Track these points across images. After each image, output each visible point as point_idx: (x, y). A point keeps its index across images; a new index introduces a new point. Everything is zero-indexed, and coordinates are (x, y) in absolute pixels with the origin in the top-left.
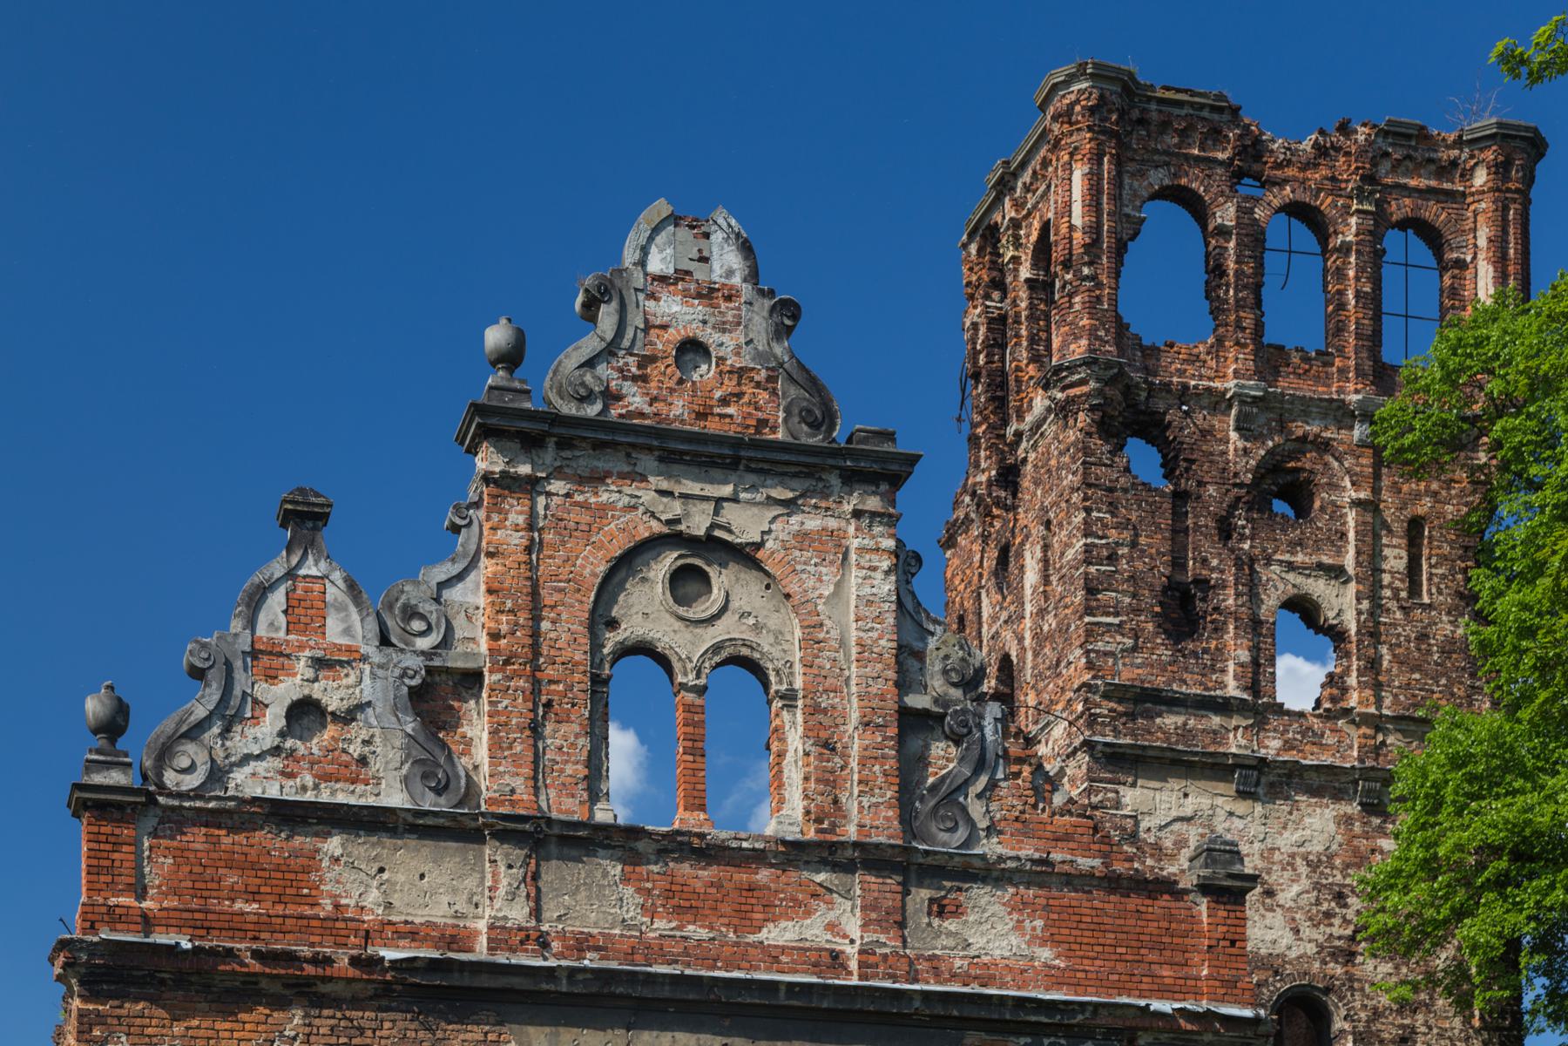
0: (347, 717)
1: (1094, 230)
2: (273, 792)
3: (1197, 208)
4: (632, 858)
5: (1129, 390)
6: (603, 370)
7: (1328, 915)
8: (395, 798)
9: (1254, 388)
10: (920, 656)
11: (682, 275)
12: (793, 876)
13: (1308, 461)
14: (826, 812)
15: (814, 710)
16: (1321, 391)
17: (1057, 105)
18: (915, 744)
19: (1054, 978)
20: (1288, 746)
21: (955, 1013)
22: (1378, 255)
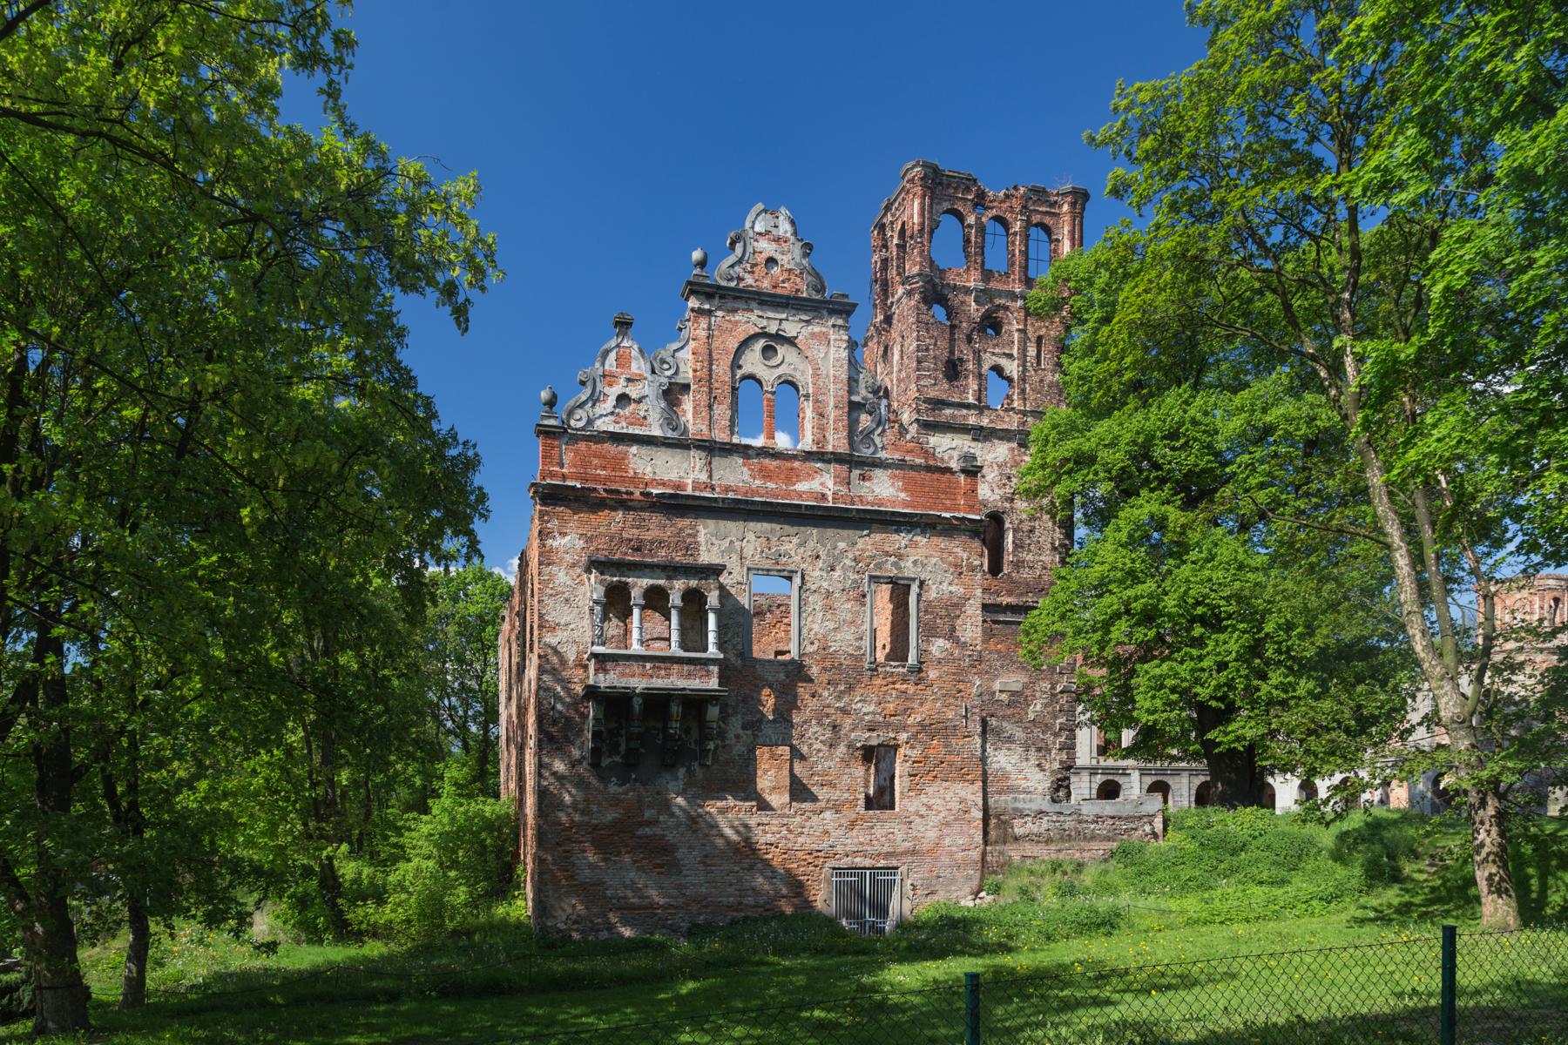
0: (639, 401)
1: (922, 224)
2: (611, 429)
3: (960, 217)
4: (747, 457)
5: (934, 286)
6: (737, 269)
8: (657, 432)
9: (981, 286)
10: (857, 381)
11: (768, 232)
12: (808, 464)
13: (1001, 314)
14: (821, 440)
15: (816, 401)
16: (1006, 288)
17: (909, 176)
18: (854, 415)
19: (906, 504)
20: (991, 421)
22: (1028, 236)
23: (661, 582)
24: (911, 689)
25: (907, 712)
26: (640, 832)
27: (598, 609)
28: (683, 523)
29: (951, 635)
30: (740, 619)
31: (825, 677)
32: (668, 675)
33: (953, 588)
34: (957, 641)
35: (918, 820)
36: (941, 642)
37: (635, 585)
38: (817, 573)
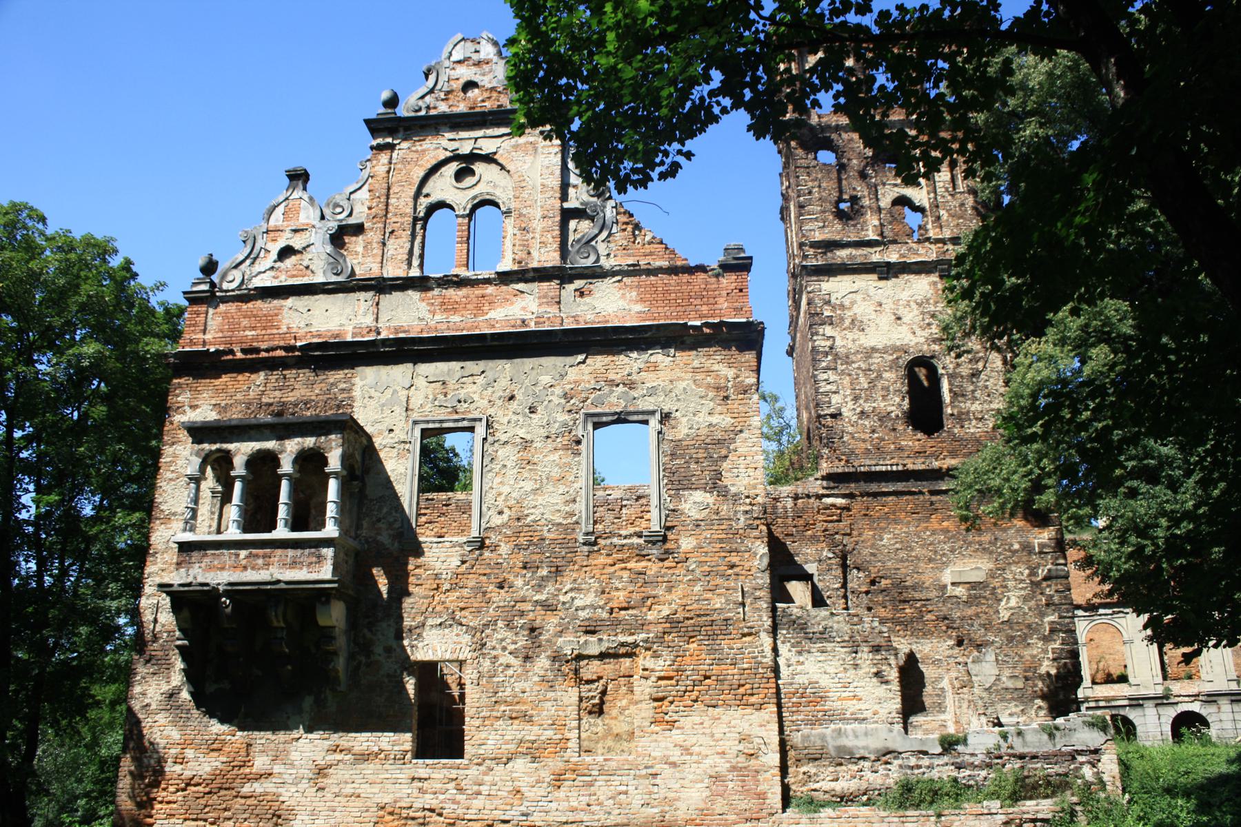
7: (929, 324)
8: (319, 278)
21: (581, 339)
24: (653, 568)
25: (647, 601)
26: (246, 789)
28: (335, 376)
29: (715, 485)
33: (714, 419)
34: (723, 493)
35: (667, 771)
36: (699, 496)
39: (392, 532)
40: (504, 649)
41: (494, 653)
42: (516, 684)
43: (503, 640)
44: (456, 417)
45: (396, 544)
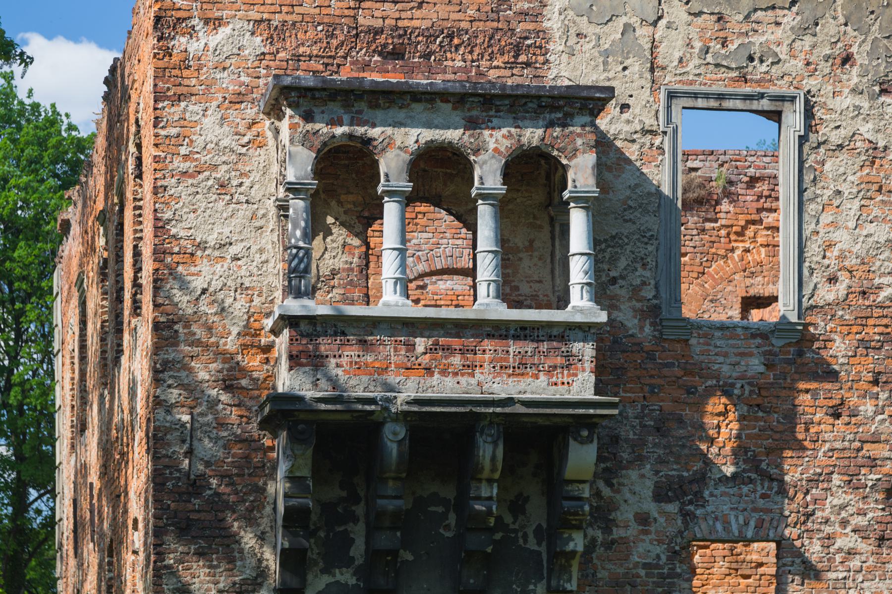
23: (453, 135)
27: (298, 205)
30: (651, 222)
31: (865, 367)
32: (470, 368)
37: (389, 143)
38: (846, 101)
39: (638, 305)
40: (844, 523)
41: (828, 529)
42: (866, 584)
43: (843, 507)
44: (747, 89)
45: (648, 329)
